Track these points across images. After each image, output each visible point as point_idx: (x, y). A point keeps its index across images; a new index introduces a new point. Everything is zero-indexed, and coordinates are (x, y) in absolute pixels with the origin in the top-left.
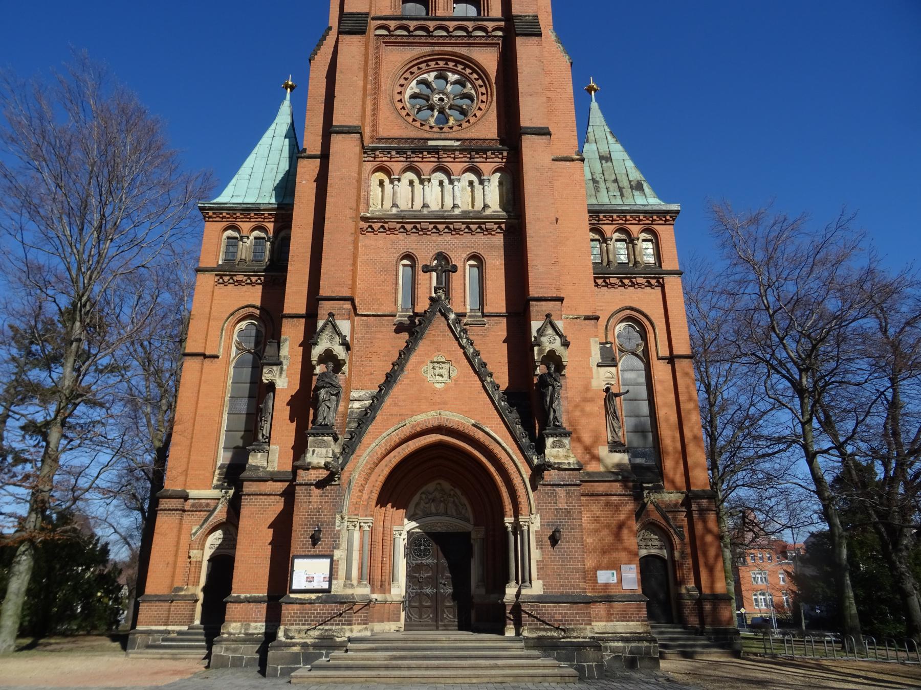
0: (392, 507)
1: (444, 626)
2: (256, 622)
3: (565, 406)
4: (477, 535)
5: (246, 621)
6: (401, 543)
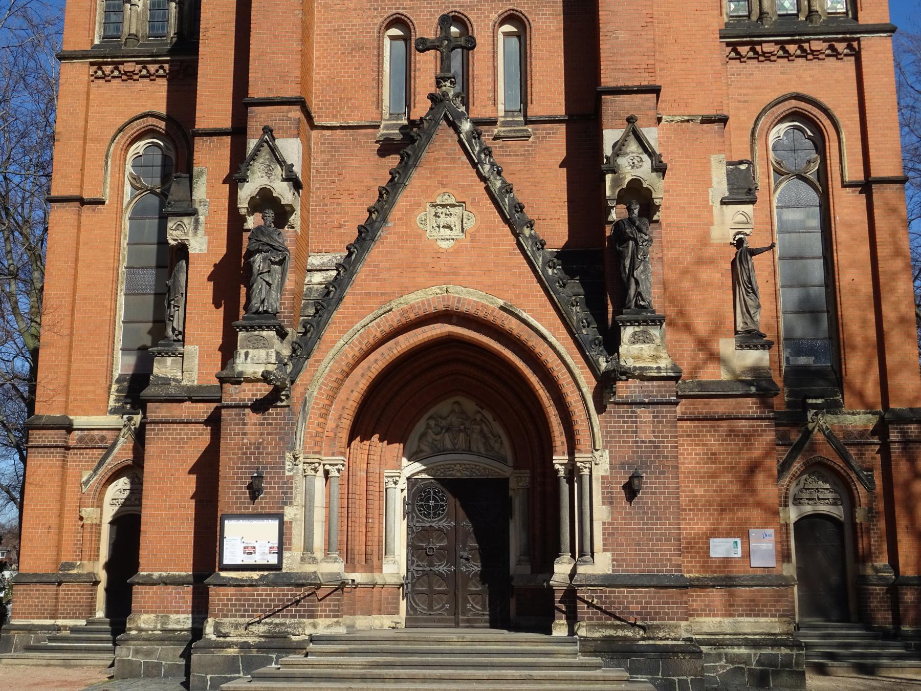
0: (381, 440)
1: (468, 621)
2: (178, 613)
3: (656, 273)
4: (518, 484)
5: (163, 612)
6: (398, 496)
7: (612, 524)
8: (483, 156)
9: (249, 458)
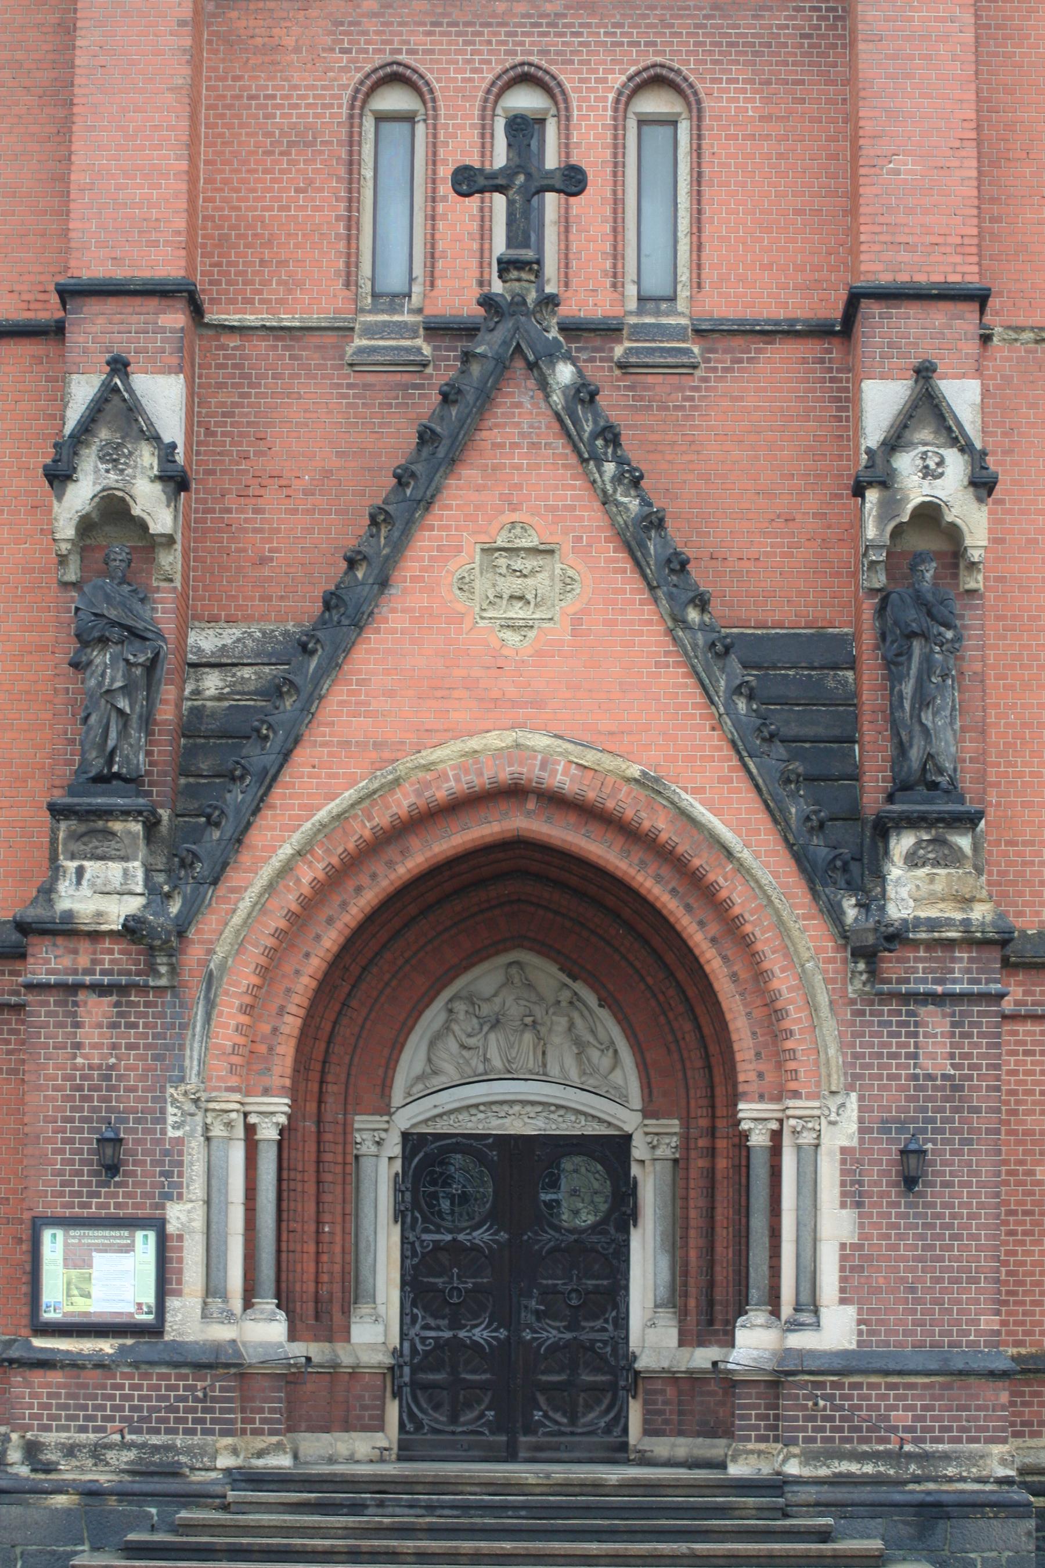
1: (538, 1448)
7: (859, 1247)
8: (599, 443)
9: (90, 1099)
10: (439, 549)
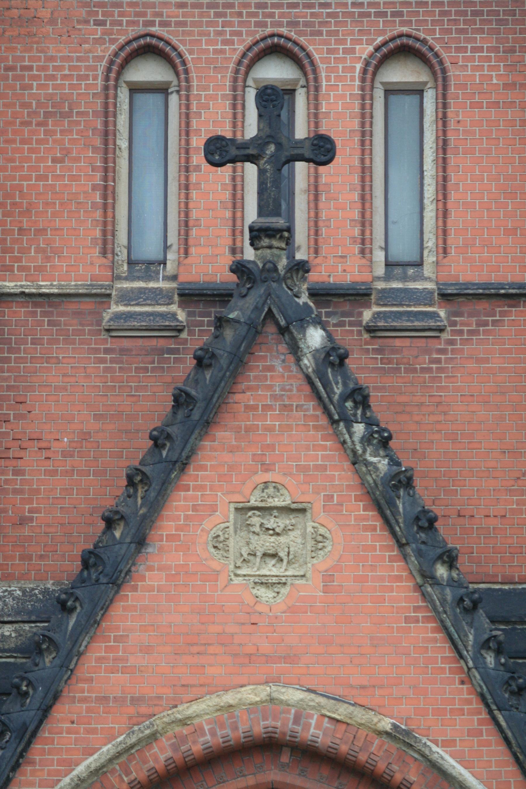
8: (349, 404)
10: (195, 508)
